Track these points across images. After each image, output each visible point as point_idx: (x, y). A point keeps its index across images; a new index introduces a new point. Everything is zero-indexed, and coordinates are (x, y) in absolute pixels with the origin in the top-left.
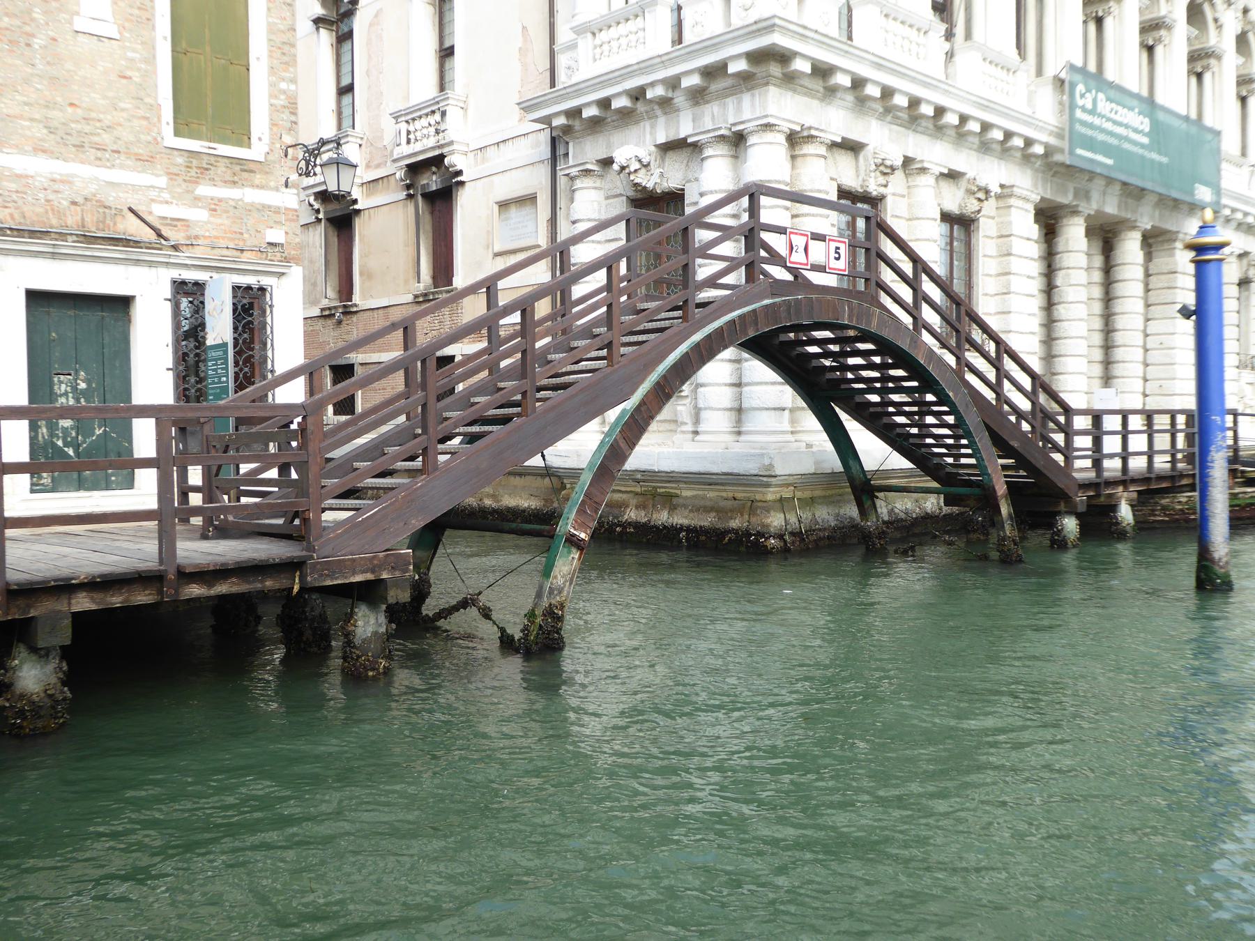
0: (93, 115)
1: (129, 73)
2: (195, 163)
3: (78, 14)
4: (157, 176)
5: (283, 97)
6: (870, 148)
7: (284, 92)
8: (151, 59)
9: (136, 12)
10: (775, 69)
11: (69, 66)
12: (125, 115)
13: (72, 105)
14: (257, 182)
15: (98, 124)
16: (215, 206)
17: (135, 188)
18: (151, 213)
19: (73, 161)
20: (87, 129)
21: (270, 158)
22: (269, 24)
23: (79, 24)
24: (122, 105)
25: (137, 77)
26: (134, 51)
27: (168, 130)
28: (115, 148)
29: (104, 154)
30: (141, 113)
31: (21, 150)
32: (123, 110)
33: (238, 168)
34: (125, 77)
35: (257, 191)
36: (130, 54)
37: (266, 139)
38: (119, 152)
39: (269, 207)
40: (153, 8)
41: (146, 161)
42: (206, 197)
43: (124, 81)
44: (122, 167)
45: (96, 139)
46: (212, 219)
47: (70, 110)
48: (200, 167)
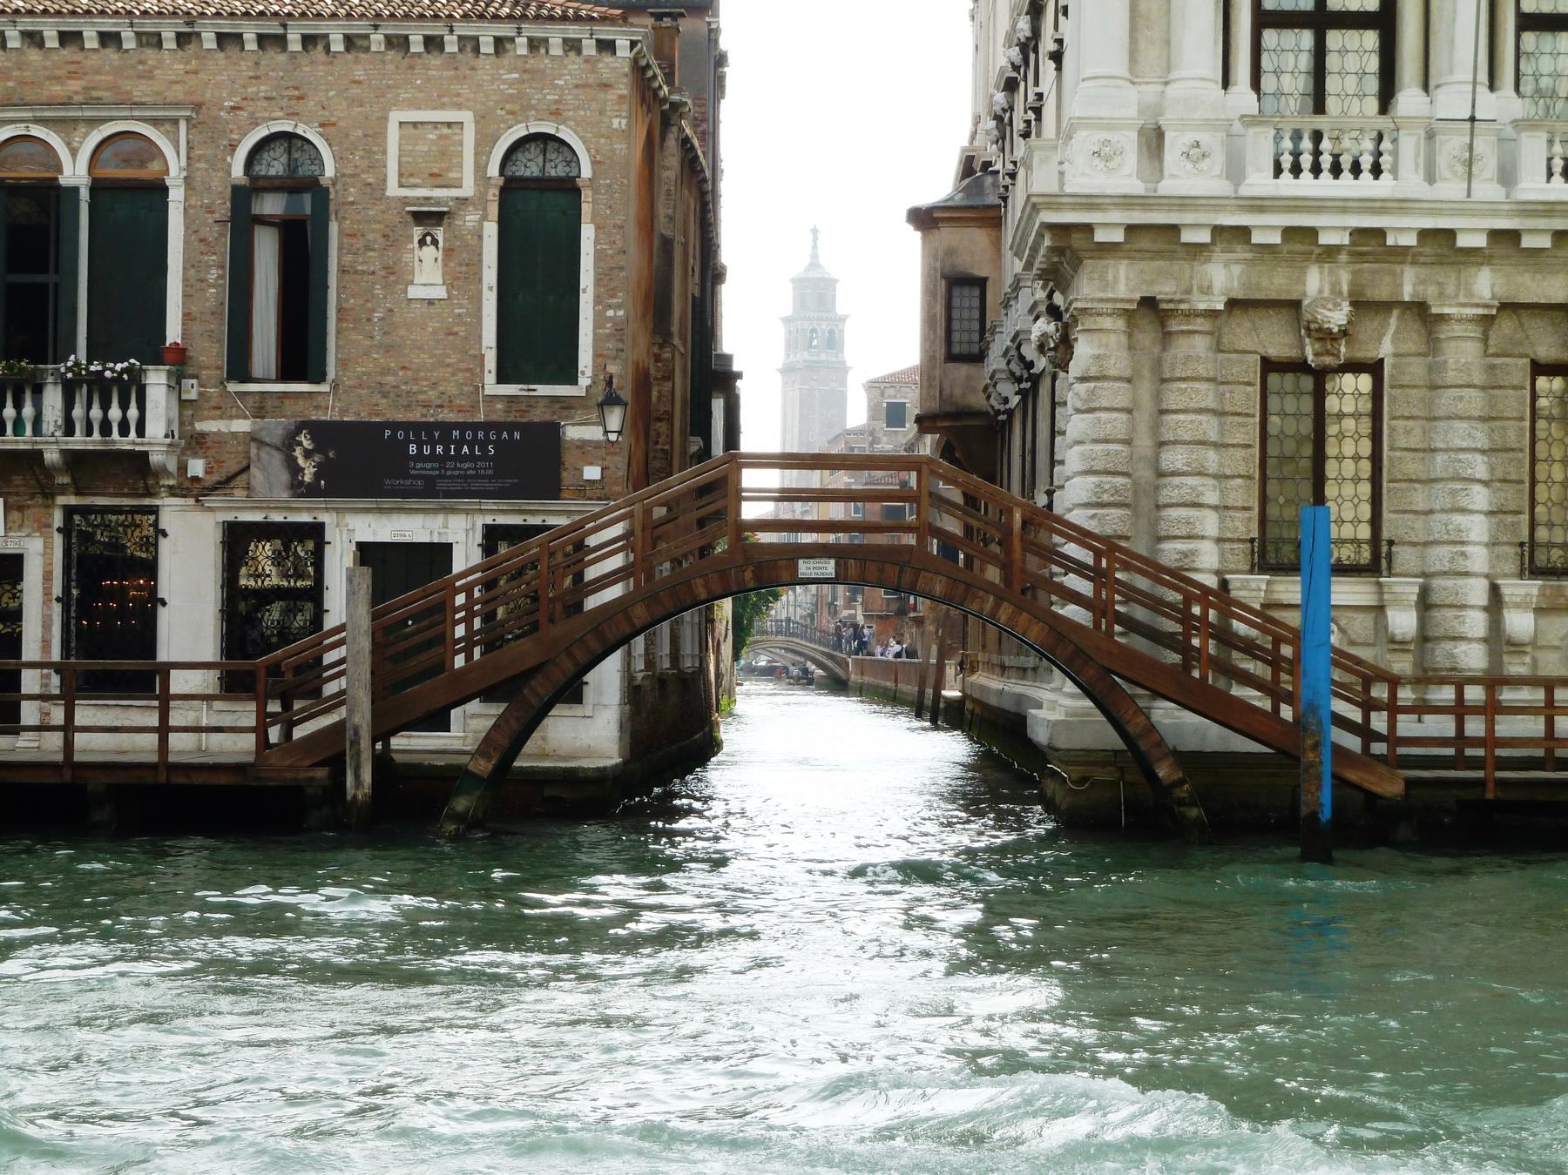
2: (515, 406)
3: (412, 283)
6: (1306, 303)
9: (464, 269)
10: (1077, 241)
11: (402, 333)
13: (404, 368)
20: (415, 388)
21: (593, 390)
22: (596, 251)
23: (413, 292)
24: (448, 361)
27: (490, 378)
30: (463, 365)
33: (557, 406)
37: (589, 372)
38: (441, 406)
40: (480, 261)
45: (421, 397)
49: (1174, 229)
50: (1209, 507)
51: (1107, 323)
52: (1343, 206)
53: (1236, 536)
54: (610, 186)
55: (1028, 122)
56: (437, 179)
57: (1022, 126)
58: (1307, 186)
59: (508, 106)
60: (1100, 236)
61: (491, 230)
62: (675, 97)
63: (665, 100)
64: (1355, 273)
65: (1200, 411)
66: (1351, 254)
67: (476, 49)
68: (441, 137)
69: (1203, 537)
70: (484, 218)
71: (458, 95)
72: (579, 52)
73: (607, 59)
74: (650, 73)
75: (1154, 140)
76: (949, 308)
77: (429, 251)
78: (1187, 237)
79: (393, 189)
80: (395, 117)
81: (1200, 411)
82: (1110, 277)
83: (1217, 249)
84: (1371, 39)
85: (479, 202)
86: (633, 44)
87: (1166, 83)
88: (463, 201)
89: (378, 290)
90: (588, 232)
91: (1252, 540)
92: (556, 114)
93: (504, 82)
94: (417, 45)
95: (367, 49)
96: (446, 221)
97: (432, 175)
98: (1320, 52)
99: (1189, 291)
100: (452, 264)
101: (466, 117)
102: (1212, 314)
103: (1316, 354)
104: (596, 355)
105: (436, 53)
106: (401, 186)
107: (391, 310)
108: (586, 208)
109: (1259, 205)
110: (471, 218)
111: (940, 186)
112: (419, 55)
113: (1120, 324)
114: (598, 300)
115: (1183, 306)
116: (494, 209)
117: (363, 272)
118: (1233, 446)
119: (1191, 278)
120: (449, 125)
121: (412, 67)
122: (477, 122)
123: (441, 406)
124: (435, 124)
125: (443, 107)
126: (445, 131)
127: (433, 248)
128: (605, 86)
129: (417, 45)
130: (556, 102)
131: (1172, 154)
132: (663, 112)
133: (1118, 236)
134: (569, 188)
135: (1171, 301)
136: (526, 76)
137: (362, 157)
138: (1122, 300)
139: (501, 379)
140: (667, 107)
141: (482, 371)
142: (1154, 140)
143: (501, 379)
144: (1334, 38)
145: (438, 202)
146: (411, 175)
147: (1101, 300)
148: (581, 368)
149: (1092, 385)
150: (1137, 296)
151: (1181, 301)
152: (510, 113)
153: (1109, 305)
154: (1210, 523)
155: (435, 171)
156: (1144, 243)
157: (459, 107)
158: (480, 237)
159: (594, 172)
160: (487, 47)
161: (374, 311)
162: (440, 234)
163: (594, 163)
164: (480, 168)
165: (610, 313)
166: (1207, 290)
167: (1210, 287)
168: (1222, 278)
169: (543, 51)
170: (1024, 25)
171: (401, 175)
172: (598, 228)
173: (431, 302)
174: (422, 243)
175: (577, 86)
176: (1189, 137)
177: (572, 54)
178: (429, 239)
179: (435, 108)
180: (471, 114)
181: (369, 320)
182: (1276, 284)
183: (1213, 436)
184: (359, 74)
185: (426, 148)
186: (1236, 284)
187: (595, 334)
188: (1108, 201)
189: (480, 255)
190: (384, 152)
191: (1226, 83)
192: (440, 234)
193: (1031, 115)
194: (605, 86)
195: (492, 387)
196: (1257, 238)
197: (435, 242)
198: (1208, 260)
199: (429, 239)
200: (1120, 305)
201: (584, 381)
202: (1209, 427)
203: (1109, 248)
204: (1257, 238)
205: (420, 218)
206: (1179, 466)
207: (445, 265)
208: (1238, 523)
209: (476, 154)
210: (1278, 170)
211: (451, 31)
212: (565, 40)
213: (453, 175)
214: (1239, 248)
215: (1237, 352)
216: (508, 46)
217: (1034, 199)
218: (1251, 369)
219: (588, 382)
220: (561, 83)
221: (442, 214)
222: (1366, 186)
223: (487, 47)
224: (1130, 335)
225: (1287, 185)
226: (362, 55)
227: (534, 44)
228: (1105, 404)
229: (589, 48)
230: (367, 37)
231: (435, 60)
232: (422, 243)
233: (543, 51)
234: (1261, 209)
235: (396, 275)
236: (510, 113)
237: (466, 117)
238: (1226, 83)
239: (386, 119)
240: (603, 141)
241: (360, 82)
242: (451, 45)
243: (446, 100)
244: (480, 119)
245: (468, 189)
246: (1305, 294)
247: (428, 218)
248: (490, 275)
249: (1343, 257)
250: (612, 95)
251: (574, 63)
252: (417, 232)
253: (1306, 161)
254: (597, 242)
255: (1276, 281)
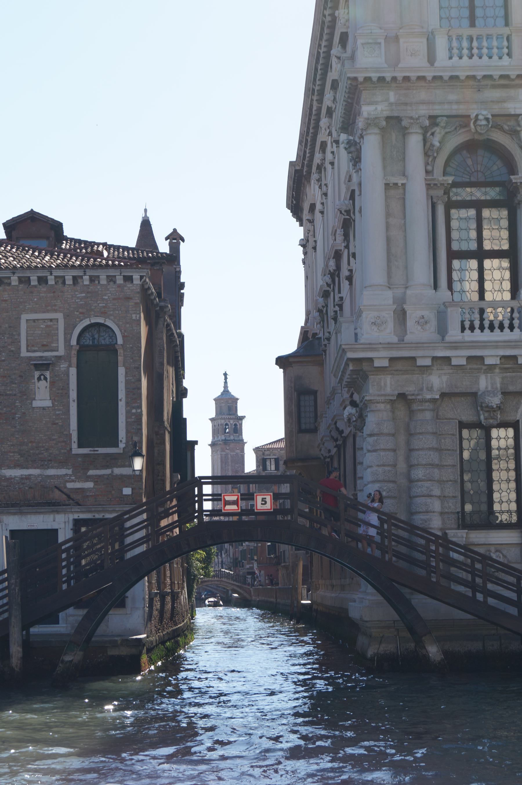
0: (41, 445)
1: (57, 421)
3: (34, 399)
4: (69, 469)
5: (133, 417)
6: (479, 393)
7: (134, 414)
8: (67, 412)
9: (61, 391)
12: (54, 442)
13: (31, 442)
14: (119, 464)
15: (42, 449)
16: (96, 479)
17: (58, 477)
18: (66, 487)
19: (31, 468)
20: (37, 452)
22: (126, 381)
23: (35, 404)
24: (54, 437)
25: (60, 422)
26: (59, 410)
27: (75, 446)
28: (50, 458)
29: (45, 464)
31: (9, 467)
32: (53, 440)
34: (55, 424)
35: (119, 469)
36: (57, 412)
37: (124, 441)
38: (51, 460)
39: (125, 475)
40: (69, 387)
41: (62, 464)
42: (93, 475)
43: (55, 426)
44: (52, 467)
46: (96, 486)
47: (30, 445)
48: (91, 461)
49: (413, 359)
50: (436, 496)
51: (382, 406)
52: (496, 345)
53: (450, 511)
54: (132, 348)
55: (336, 312)
56: (46, 347)
57: (333, 314)
58: (478, 336)
59: (80, 310)
60: (377, 364)
61: (73, 371)
62: (162, 304)
63: (157, 305)
64: (503, 378)
65: (429, 449)
66: (501, 369)
67: (64, 283)
68: (47, 326)
69: (434, 512)
70: (70, 366)
71: (55, 305)
72: (115, 282)
73: (129, 285)
74: (150, 292)
75: (401, 316)
76: (299, 406)
77: (43, 383)
78: (420, 362)
79: (24, 353)
80: (25, 317)
81: (429, 449)
82: (383, 384)
83: (435, 368)
84: (506, 263)
85: (66, 358)
86: (141, 277)
87: (406, 288)
88: (59, 358)
89: (18, 404)
90: (121, 371)
91: (458, 513)
92: (104, 314)
93: (78, 298)
94: (34, 281)
95: (9, 284)
96: (51, 368)
97: (43, 345)
98: (481, 270)
99: (422, 389)
100: (54, 389)
101: (59, 316)
102: (433, 401)
103: (486, 419)
104: (127, 432)
105: (44, 285)
106: (28, 351)
107: (24, 413)
108: (120, 359)
109: (455, 346)
110: (63, 366)
111: (290, 345)
112: (35, 286)
113: (389, 407)
114: (127, 404)
115: (419, 397)
116: (74, 361)
117: (10, 395)
118: (447, 466)
119: (423, 383)
120: (51, 320)
121: (32, 292)
122: (65, 318)
123: (51, 460)
124: (44, 320)
125: (48, 311)
126: (49, 323)
127: (44, 381)
128: (128, 298)
129: (34, 281)
130: (104, 307)
131: (410, 323)
132: (156, 311)
133: (386, 363)
134: (112, 349)
135: (413, 395)
136: (89, 295)
137: (8, 338)
138: (389, 395)
139: (80, 446)
140: (158, 308)
141: (71, 442)
142: (401, 316)
143: (80, 446)
144: (487, 263)
145: (46, 358)
146: (33, 346)
147: (379, 395)
148: (120, 439)
149: (376, 438)
150: (396, 393)
151: (418, 395)
152: (81, 313)
153: (383, 398)
154: (437, 505)
155: (45, 343)
156: (399, 366)
157: (56, 311)
158: (68, 375)
159: (124, 341)
160: (69, 281)
161: (16, 414)
162: (48, 374)
163: (124, 337)
164: (67, 341)
165: (134, 411)
166: (430, 389)
167: (432, 387)
168: (438, 381)
169: (97, 282)
170: (332, 264)
171: (28, 346)
172: (126, 369)
173: (44, 408)
174: (39, 379)
175: (114, 299)
176: (419, 313)
177: (112, 283)
178: (42, 377)
179: (44, 312)
180: (62, 314)
181: (13, 418)
182: (464, 384)
183: (436, 461)
184: (6, 296)
185: (40, 332)
186: (445, 385)
187: (127, 422)
188: (380, 346)
189: (68, 384)
190: (19, 335)
191: (436, 287)
192: (48, 374)
193: (337, 308)
194: (128, 298)
195: (76, 450)
196: (454, 362)
197: (46, 379)
198: (430, 374)
199: (42, 377)
200: (387, 398)
201: (122, 445)
202: (434, 457)
203: (382, 370)
204: (454, 362)
205: (37, 367)
206: (420, 476)
207: (51, 389)
208: (450, 504)
209: (65, 334)
210: (463, 329)
211: (51, 274)
212: (108, 276)
213: (54, 345)
214: (445, 368)
215: (446, 419)
216: (79, 280)
217: (343, 347)
218: (454, 428)
219: (124, 445)
220: (106, 297)
221: (49, 364)
222: (507, 335)
223: (69, 281)
224: (393, 412)
225: (468, 335)
226: (7, 287)
227: (92, 279)
228: (382, 447)
229: (120, 280)
230: (9, 278)
231: (43, 289)
232: (39, 379)
233: (97, 282)
234: (456, 348)
235: (27, 395)
236: (81, 313)
237: (59, 316)
238: (436, 287)
239: (20, 318)
240: (128, 326)
241: (6, 301)
242: (51, 281)
243: (49, 308)
244: (66, 317)
245: (61, 352)
246: (479, 389)
247: (43, 366)
248: (73, 395)
249: (497, 370)
250: (131, 303)
251: (112, 288)
252: (37, 374)
253: (477, 324)
254: (126, 376)
255: (464, 383)
